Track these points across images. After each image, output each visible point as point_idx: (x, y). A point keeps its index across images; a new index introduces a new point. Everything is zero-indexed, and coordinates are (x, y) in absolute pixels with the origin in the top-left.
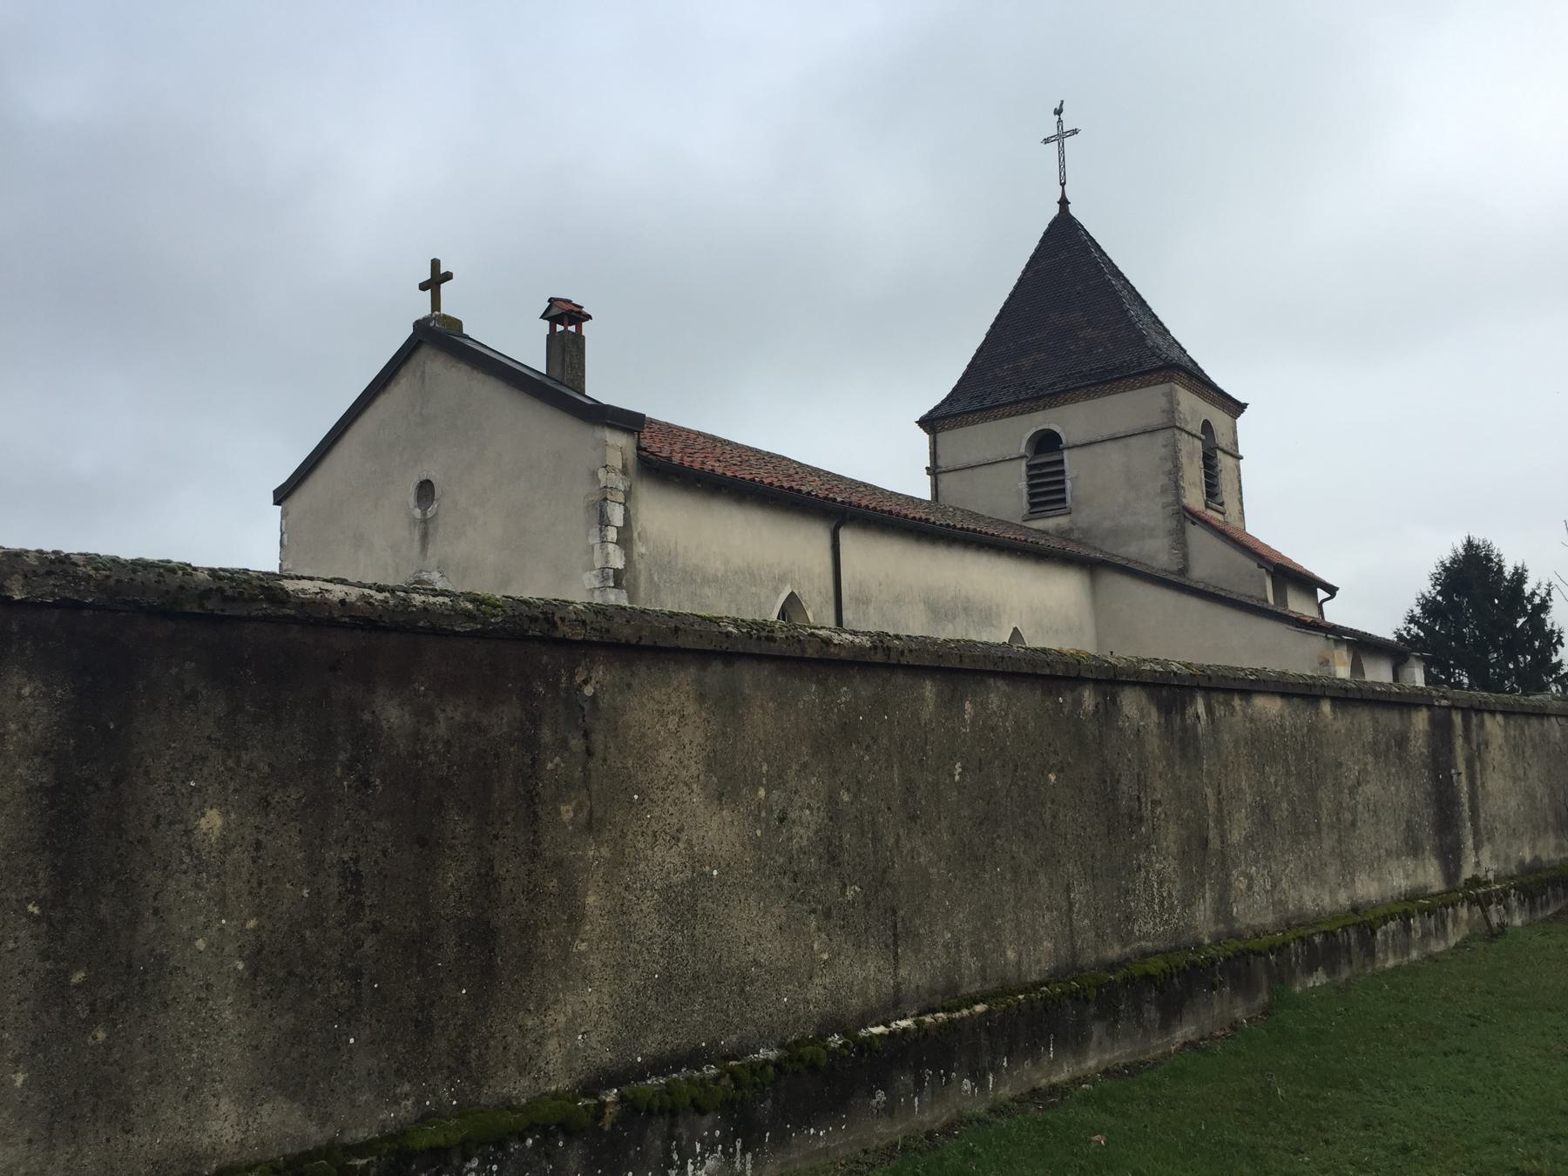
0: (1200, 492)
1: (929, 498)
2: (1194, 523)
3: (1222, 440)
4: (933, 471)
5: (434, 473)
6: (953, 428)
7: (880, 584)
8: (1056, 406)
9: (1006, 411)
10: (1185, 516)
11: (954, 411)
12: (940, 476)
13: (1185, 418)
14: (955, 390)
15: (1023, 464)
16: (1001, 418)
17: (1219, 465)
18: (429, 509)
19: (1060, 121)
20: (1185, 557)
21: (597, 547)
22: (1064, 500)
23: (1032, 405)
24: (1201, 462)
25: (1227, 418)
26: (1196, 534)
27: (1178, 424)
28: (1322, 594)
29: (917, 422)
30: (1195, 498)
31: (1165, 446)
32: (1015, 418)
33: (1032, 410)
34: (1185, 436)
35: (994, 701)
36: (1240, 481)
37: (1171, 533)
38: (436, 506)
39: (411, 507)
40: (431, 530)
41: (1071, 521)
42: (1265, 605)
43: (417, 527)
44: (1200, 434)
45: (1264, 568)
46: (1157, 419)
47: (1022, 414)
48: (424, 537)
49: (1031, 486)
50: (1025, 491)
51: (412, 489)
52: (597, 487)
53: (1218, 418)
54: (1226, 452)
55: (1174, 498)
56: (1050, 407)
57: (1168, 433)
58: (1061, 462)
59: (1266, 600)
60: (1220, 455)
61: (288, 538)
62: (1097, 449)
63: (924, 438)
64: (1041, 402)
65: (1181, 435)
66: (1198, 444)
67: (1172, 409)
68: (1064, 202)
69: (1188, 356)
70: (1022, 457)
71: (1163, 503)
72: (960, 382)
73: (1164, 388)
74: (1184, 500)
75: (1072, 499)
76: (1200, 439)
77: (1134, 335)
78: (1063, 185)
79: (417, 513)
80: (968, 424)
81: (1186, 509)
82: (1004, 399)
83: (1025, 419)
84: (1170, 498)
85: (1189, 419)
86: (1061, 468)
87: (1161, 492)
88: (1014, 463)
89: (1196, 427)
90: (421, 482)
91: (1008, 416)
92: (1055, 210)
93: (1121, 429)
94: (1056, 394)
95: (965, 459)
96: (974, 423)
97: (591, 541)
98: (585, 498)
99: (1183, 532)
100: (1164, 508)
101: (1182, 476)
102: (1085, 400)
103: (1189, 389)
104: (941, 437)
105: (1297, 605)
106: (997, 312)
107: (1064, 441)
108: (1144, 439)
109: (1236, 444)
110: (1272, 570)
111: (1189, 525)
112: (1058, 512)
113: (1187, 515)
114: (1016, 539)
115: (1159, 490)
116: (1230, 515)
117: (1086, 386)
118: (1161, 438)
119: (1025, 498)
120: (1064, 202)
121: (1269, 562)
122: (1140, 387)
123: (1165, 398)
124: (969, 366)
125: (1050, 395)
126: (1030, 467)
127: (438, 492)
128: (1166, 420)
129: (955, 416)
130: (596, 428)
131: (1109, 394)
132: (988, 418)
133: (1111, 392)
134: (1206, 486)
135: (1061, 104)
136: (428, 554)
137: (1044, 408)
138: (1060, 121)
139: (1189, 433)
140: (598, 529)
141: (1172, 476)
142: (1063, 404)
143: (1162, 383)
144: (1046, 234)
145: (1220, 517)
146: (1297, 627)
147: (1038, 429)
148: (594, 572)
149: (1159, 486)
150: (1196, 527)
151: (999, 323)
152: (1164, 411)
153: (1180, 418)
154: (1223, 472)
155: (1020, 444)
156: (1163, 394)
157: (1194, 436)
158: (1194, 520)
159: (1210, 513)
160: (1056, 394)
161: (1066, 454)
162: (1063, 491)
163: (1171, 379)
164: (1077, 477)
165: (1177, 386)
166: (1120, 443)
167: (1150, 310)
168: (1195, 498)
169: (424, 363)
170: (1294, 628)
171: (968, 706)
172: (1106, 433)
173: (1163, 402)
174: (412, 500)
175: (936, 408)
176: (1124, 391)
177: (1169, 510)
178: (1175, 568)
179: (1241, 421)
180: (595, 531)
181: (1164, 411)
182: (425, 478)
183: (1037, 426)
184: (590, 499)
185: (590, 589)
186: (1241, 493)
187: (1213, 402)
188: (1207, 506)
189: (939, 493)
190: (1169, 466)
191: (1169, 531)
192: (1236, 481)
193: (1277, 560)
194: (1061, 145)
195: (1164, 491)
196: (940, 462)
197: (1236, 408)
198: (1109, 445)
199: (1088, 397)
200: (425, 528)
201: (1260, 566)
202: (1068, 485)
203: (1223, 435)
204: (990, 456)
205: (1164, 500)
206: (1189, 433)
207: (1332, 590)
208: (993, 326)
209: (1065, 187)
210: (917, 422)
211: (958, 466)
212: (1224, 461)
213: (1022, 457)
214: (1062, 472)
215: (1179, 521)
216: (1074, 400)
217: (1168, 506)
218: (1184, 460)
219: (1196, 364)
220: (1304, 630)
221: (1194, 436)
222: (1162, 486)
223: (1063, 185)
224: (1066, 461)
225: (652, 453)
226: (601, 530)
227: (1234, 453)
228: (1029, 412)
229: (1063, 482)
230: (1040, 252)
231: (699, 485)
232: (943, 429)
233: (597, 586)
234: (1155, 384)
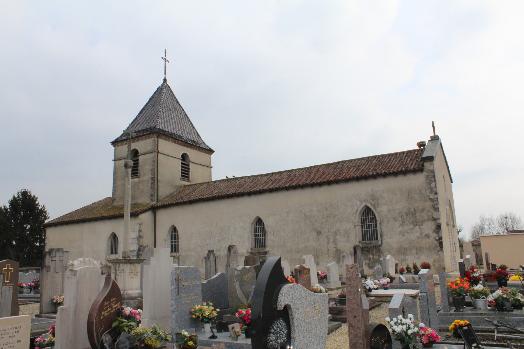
16: (176, 143)
33: (184, 146)
62: (197, 165)
68: (165, 80)
78: (165, 74)
80: (168, 140)
96: (170, 141)
112: (186, 180)
120: (165, 80)
135: (165, 50)
198: (200, 166)
199: (196, 150)
209: (166, 75)
216: (193, 148)
223: (165, 74)
224: (190, 166)
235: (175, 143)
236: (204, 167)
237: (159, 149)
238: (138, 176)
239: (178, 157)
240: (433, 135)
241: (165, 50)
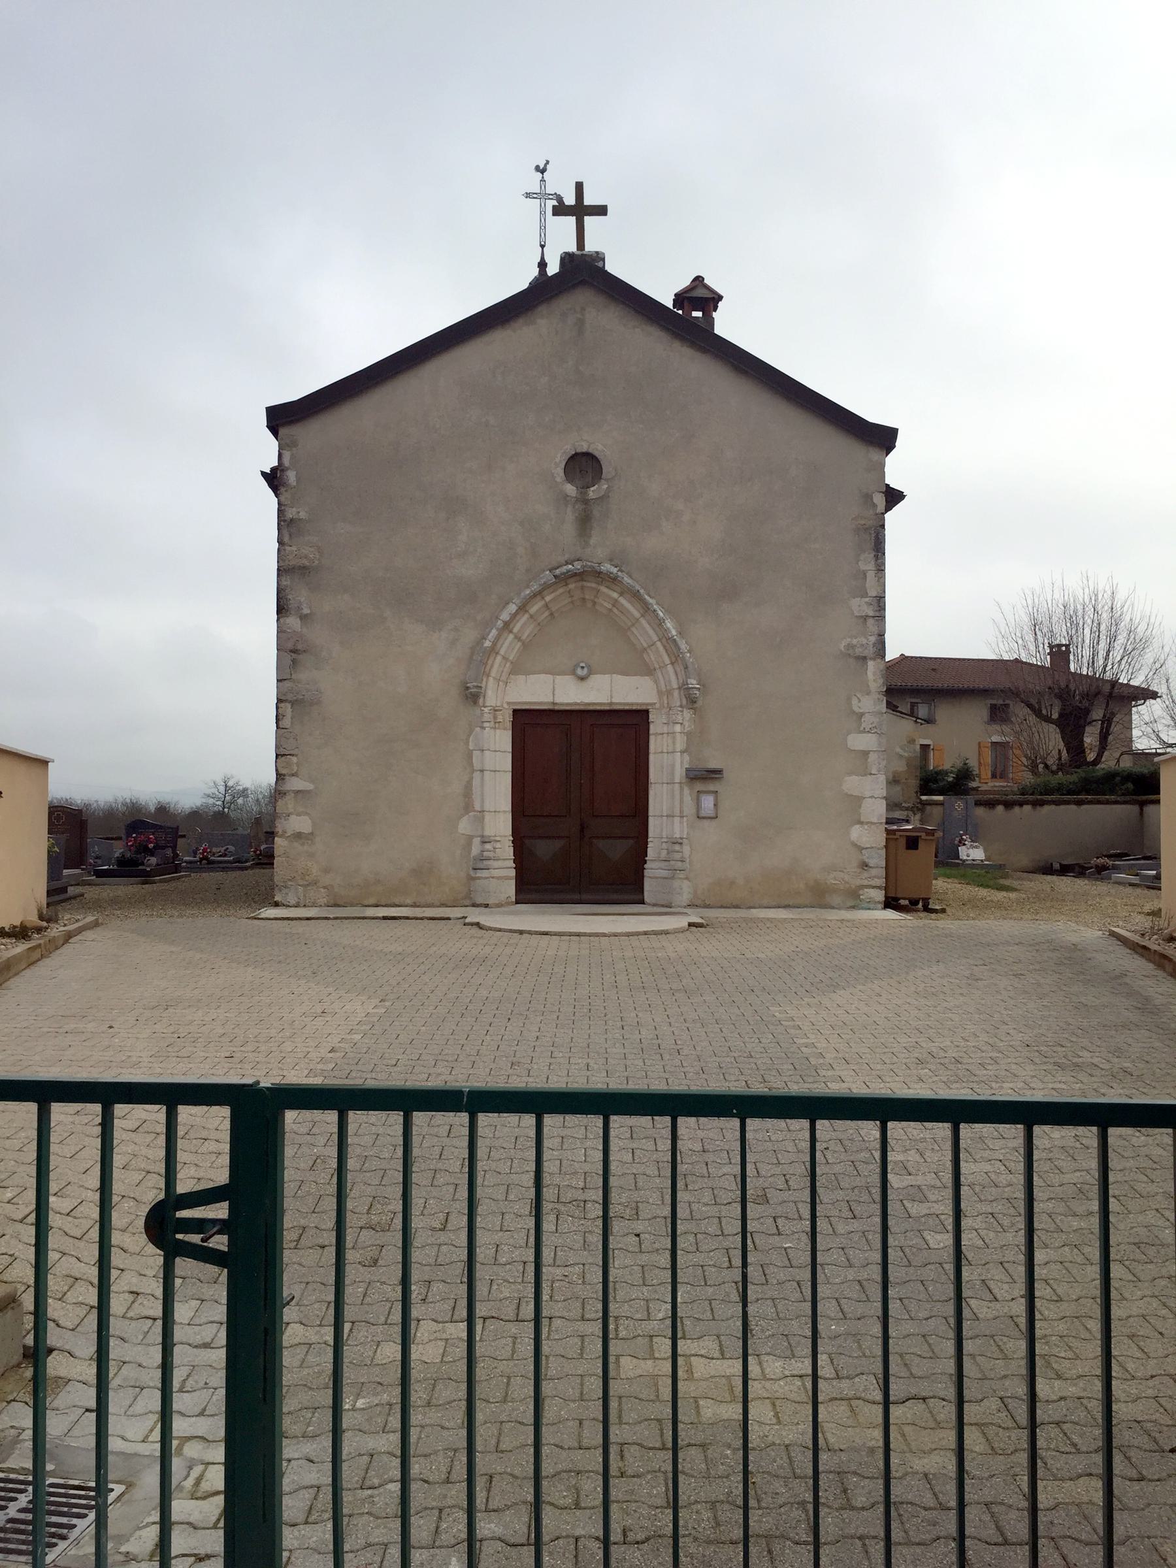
5: (600, 447)
18: (592, 489)
19: (543, 180)
21: (871, 575)
38: (605, 486)
39: (558, 479)
40: (596, 512)
43: (569, 509)
48: (585, 522)
51: (561, 459)
52: (871, 512)
61: (298, 480)
78: (543, 246)
79: (570, 489)
90: (576, 454)
92: (535, 272)
97: (863, 566)
98: (852, 520)
127: (607, 470)
130: (871, 449)
136: (592, 541)
138: (543, 180)
140: (872, 555)
148: (867, 599)
169: (583, 309)
170: (891, 712)
174: (559, 472)
180: (870, 556)
182: (584, 450)
184: (863, 522)
185: (862, 617)
200: (585, 510)
223: (543, 246)
226: (877, 557)
233: (871, 613)
240: (572, 248)
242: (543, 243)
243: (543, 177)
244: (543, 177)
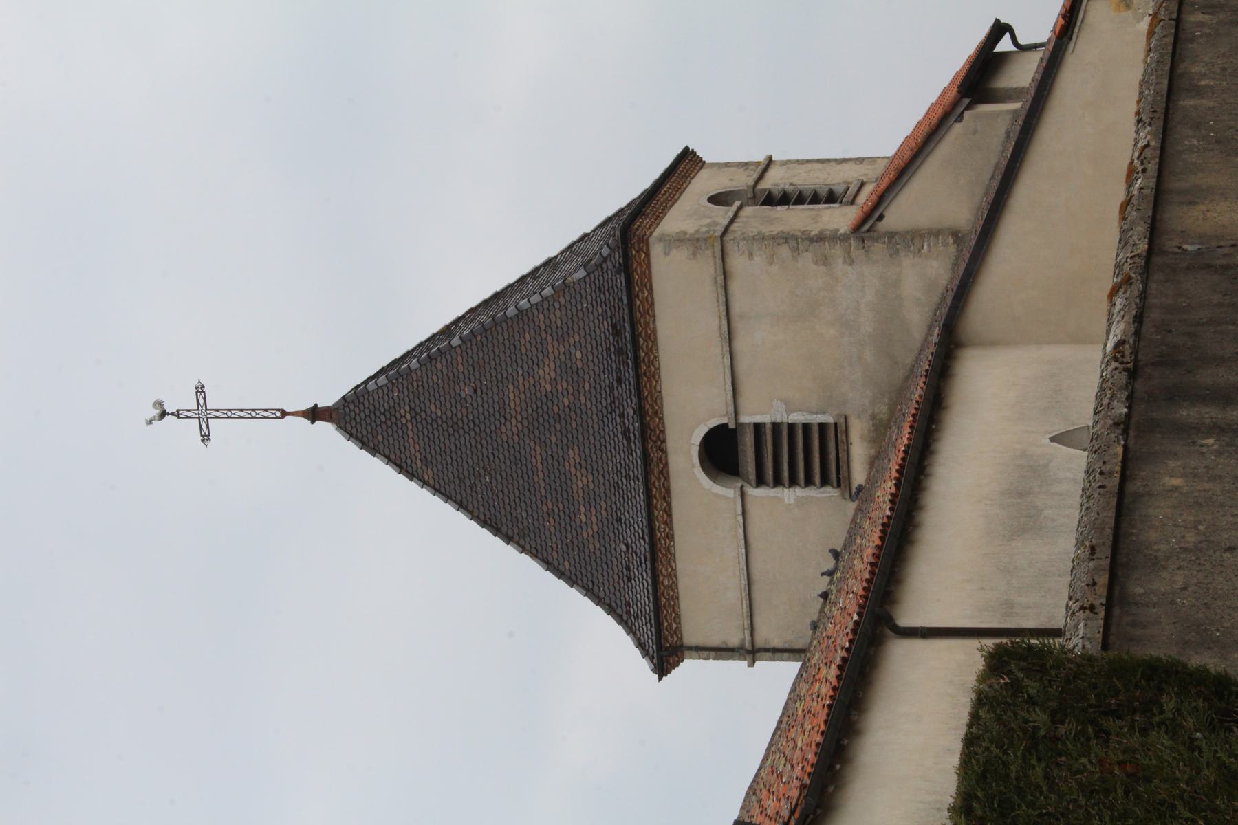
0: (828, 212)
1: (789, 669)
2: (881, 218)
3: (743, 181)
4: (752, 652)
6: (678, 616)
7: (982, 589)
8: (663, 432)
9: (660, 519)
10: (868, 231)
11: (649, 608)
12: (760, 643)
13: (707, 225)
14: (610, 610)
15: (755, 493)
16: (671, 529)
17: (782, 186)
19: (177, 414)
20: (935, 233)
22: (822, 427)
23: (656, 471)
24: (779, 208)
25: (704, 174)
26: (898, 215)
27: (718, 234)
28: (1005, 45)
29: (660, 679)
30: (840, 218)
31: (751, 255)
32: (674, 504)
33: (665, 473)
34: (734, 227)
35: (1196, 69)
36: (808, 161)
37: (895, 253)
41: (859, 417)
42: (1024, 113)
44: (734, 208)
45: (962, 113)
46: (706, 267)
47: (668, 491)
49: (793, 482)
50: (799, 492)
53: (701, 186)
54: (761, 177)
55: (838, 247)
56: (664, 441)
57: (731, 247)
58: (758, 427)
59: (1015, 112)
60: (766, 184)
62: (743, 365)
63: (689, 668)
64: (654, 455)
65: (734, 231)
66: (749, 211)
67: (694, 242)
68: (314, 414)
69: (594, 231)
70: (743, 495)
71: (845, 262)
72: (598, 601)
73: (656, 250)
74: (842, 231)
75: (824, 413)
76: (740, 208)
77: (562, 300)
78: (284, 414)
80: (674, 586)
81: (856, 229)
82: (642, 519)
83: (678, 485)
84: (837, 251)
85: (707, 221)
86: (769, 427)
87: (825, 264)
88: (749, 507)
89: (722, 215)
91: (670, 516)
92: (326, 429)
93: (711, 322)
94: (644, 430)
95: (733, 594)
96: (673, 575)
99: (892, 235)
100: (852, 263)
101: (803, 233)
102: (658, 380)
103: (659, 218)
104: (690, 638)
105: (1022, 74)
106: (485, 533)
107: (724, 421)
108: (734, 287)
109: (745, 165)
110: (966, 101)
111: (884, 226)
113: (866, 227)
114: (911, 427)
115: (822, 268)
116: (866, 175)
117: (637, 376)
118: (738, 262)
119: (812, 492)
120: (314, 414)
121: (955, 105)
122: (651, 291)
123: (674, 252)
124: (572, 582)
125: (644, 440)
126: (760, 481)
128: (709, 253)
129: (657, 608)
131: (655, 342)
132: (668, 550)
133: (652, 338)
134: (819, 203)
137: (664, 451)
138: (177, 414)
139: (732, 221)
141: (801, 247)
142: (661, 419)
143: (648, 255)
144: (364, 445)
145: (868, 189)
146: (1071, 39)
147: (698, 464)
149: (814, 267)
150: (886, 214)
151: (504, 529)
152: (694, 255)
153: (708, 232)
154: (795, 181)
155: (717, 496)
156: (666, 254)
157: (736, 215)
158: (877, 215)
159: (862, 199)
160: (644, 430)
161: (745, 419)
162: (806, 427)
163: (644, 241)
164: (786, 402)
165: (656, 234)
166: (738, 325)
167: (510, 286)
168: (840, 218)
171: (1203, 83)
172: (717, 351)
173: (680, 255)
175: (640, 645)
176: (654, 316)
177: (856, 253)
178: (952, 249)
179: (707, 154)
181: (694, 255)
183: (693, 466)
186: (829, 160)
187: (679, 190)
188: (852, 202)
189: (786, 646)
190: (784, 251)
191: (891, 256)
192: (809, 166)
193: (954, 91)
194: (217, 414)
195: (825, 261)
196: (734, 638)
197: (687, 163)
198: (739, 345)
199: (655, 376)
201: (960, 118)
202: (798, 418)
203: (731, 180)
204: (734, 550)
205: (840, 261)
206: (732, 221)
207: (1000, 29)
208: (508, 539)
209: (287, 410)
210: (660, 679)
211: (746, 609)
212: (775, 180)
213: (743, 495)
214: (776, 426)
215: (876, 240)
216: (657, 399)
217: (849, 253)
218: (776, 229)
219: (609, 220)
220: (1076, 30)
221: (736, 215)
222: (816, 263)
223: (284, 414)
224: (758, 419)
225: (792, 813)
227: (760, 169)
228: (667, 479)
229: (791, 427)
230: (393, 457)
231: (838, 767)
232: (677, 631)
234: (649, 266)
235: (670, 537)
236: (736, 309)
237: (734, 641)
238: (841, 427)
239: (740, 518)
241: (150, 422)
242: (278, 414)
243: (173, 414)
244: (173, 414)
